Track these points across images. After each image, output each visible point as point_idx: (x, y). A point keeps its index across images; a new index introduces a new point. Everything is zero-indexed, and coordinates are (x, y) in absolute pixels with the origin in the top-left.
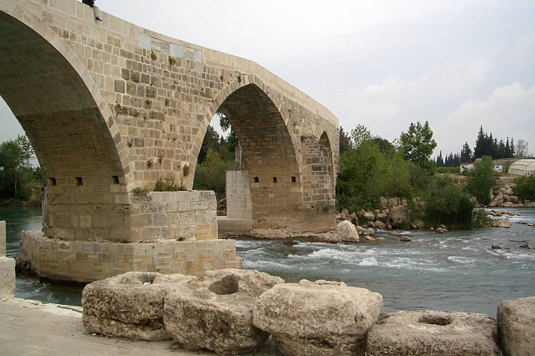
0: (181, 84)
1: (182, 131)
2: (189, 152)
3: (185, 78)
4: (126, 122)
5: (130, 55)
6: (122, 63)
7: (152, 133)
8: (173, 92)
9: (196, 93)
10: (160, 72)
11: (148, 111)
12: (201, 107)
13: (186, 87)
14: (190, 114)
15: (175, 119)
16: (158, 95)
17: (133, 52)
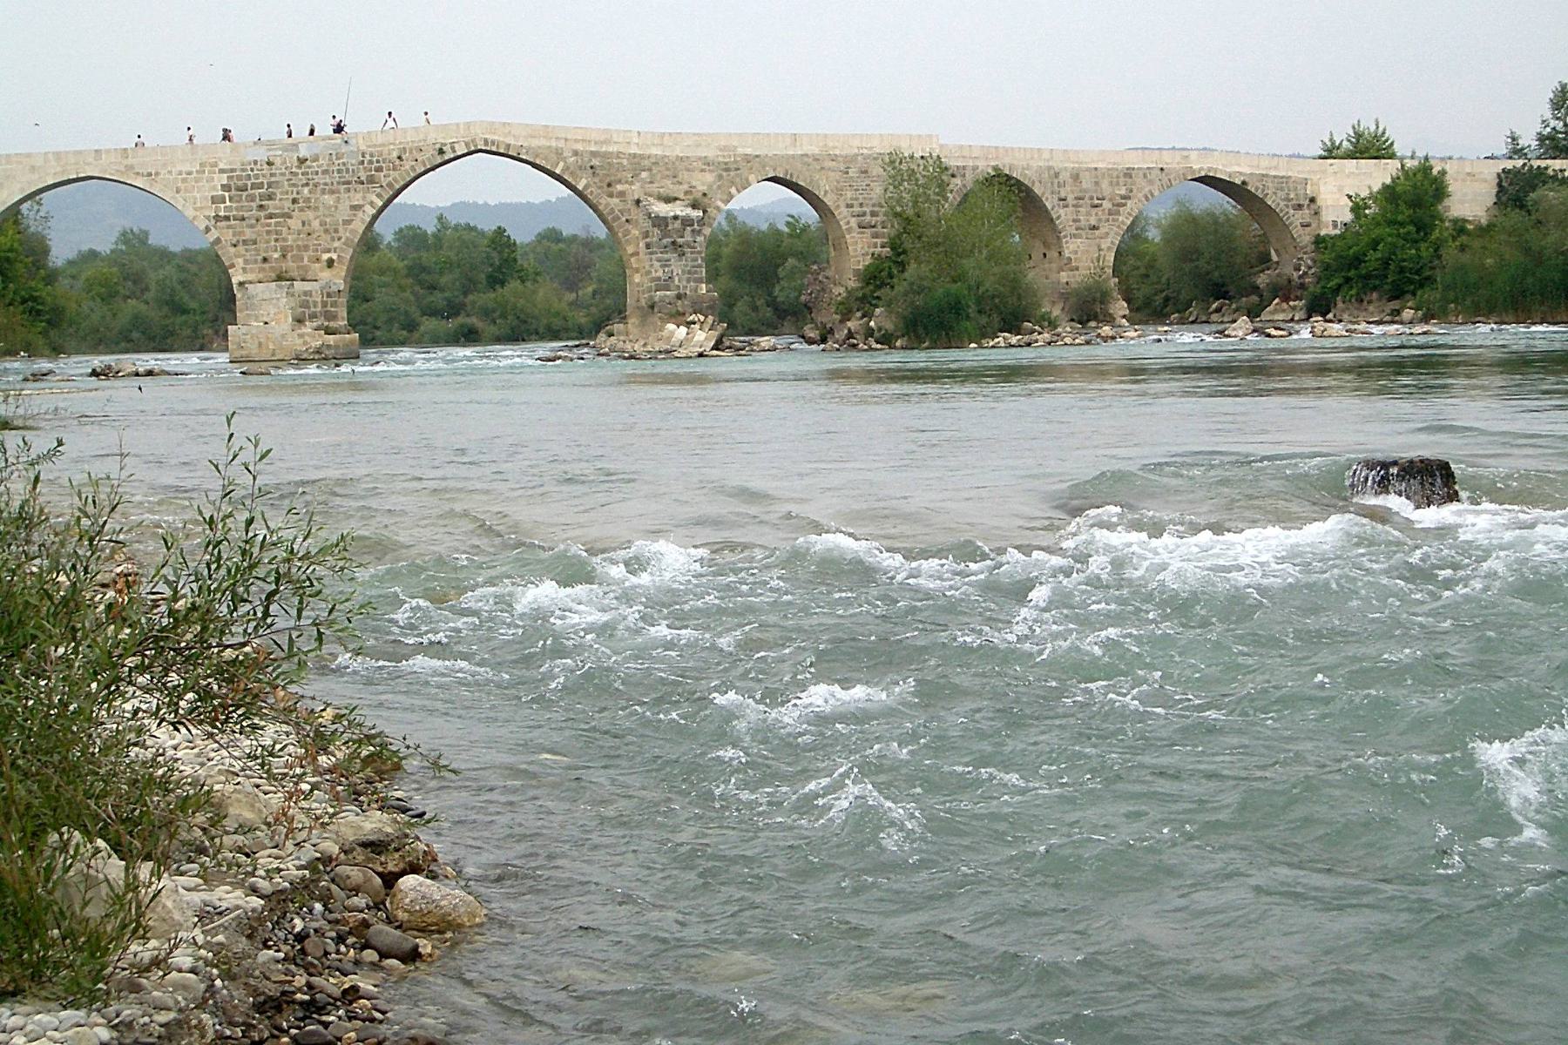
0: (319, 179)
1: (323, 224)
2: (336, 244)
3: (325, 172)
4: (229, 227)
5: (232, 170)
6: (224, 179)
7: (268, 232)
8: (306, 190)
9: (348, 183)
10: (283, 174)
11: (262, 214)
12: (359, 196)
13: (328, 181)
14: (336, 207)
15: (310, 214)
16: (279, 196)
17: (238, 166)
